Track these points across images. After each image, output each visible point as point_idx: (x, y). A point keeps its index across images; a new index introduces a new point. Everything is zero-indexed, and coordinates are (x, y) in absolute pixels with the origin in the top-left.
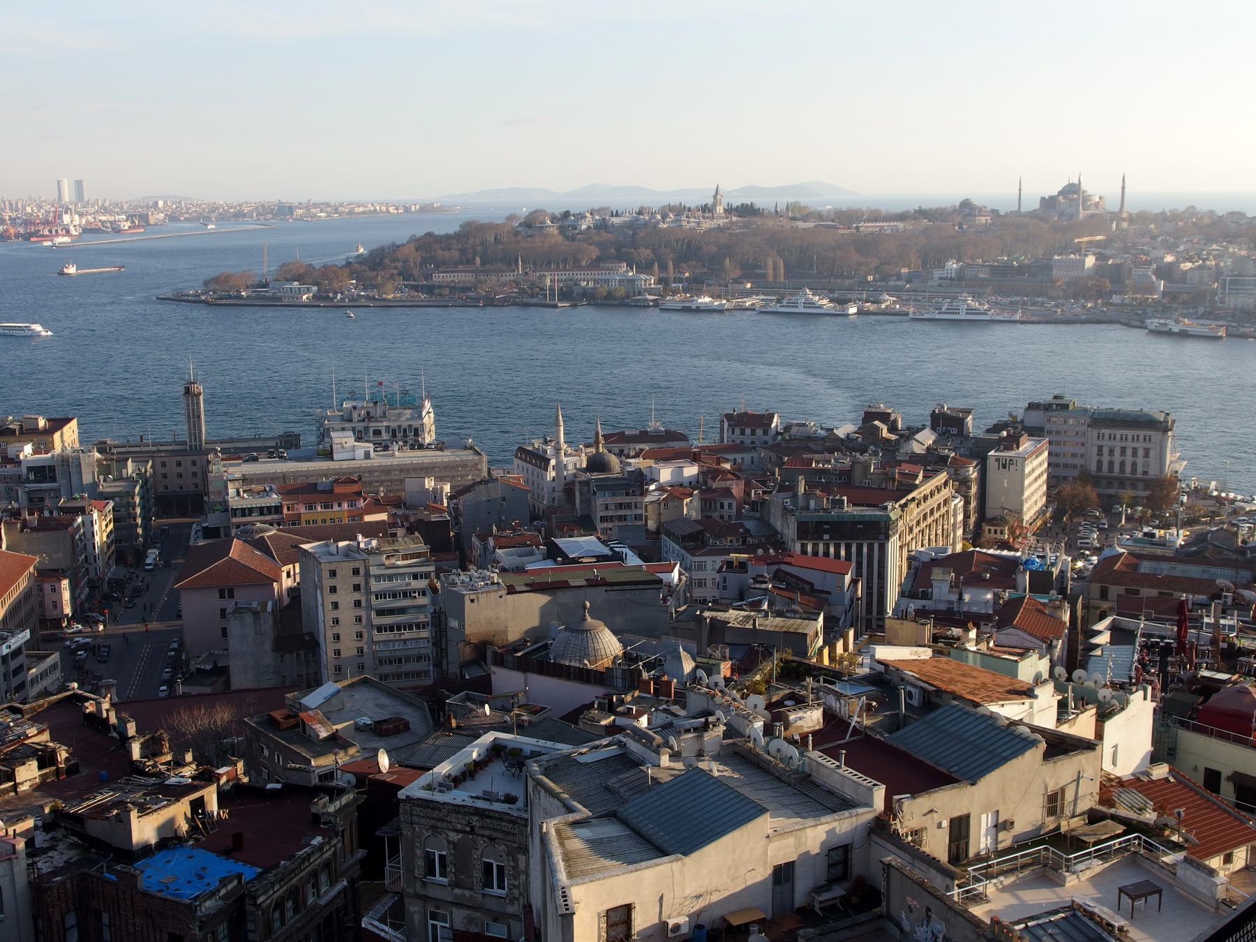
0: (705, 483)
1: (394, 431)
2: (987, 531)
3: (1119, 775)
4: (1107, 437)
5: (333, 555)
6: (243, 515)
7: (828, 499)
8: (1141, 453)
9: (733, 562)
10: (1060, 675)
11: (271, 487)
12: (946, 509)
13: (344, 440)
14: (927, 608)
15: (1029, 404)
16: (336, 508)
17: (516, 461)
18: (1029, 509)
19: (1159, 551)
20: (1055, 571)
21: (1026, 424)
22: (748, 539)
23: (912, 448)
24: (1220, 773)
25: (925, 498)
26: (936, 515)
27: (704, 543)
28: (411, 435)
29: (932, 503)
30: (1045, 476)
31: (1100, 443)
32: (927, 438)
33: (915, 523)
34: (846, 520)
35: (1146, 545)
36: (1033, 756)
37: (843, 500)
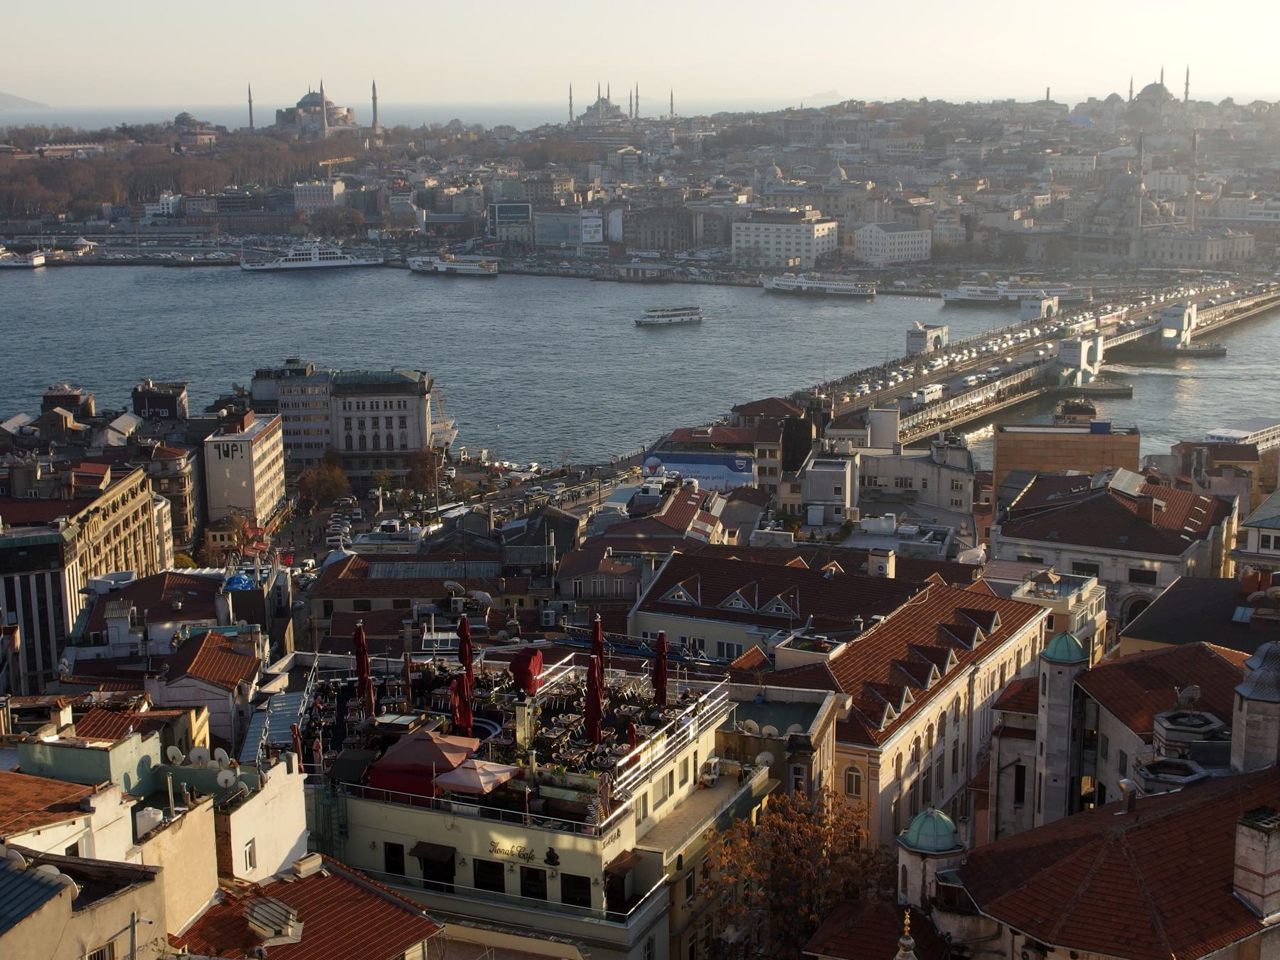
2: (211, 538)
3: (255, 881)
4: (354, 406)
8: (396, 422)
10: (174, 758)
12: (146, 517)
14: (102, 657)
15: (257, 372)
18: (264, 505)
19: (401, 549)
20: (267, 589)
21: (256, 397)
24: (401, 847)
25: (115, 507)
26: (133, 527)
29: (124, 512)
30: (281, 462)
31: (348, 414)
32: (128, 425)
33: (102, 540)
35: (384, 542)
36: (56, 910)
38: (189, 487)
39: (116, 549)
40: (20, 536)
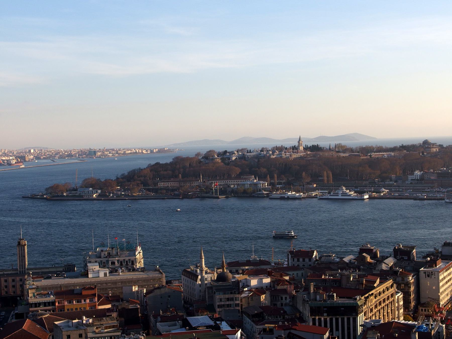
0: (274, 287)
1: (121, 262)
2: (420, 310)
5: (70, 327)
6: (36, 307)
7: (326, 295)
9: (266, 329)
11: (51, 292)
12: (392, 299)
13: (94, 267)
16: (83, 302)
17: (183, 277)
18: (444, 298)
21: (443, 253)
22: (286, 316)
23: (382, 267)
25: (380, 294)
26: (387, 302)
27: (263, 318)
28: (130, 264)
32: (390, 262)
33: (374, 306)
34: (335, 305)
37: (334, 295)
38: (412, 288)
39: (379, 310)
40: (342, 302)
